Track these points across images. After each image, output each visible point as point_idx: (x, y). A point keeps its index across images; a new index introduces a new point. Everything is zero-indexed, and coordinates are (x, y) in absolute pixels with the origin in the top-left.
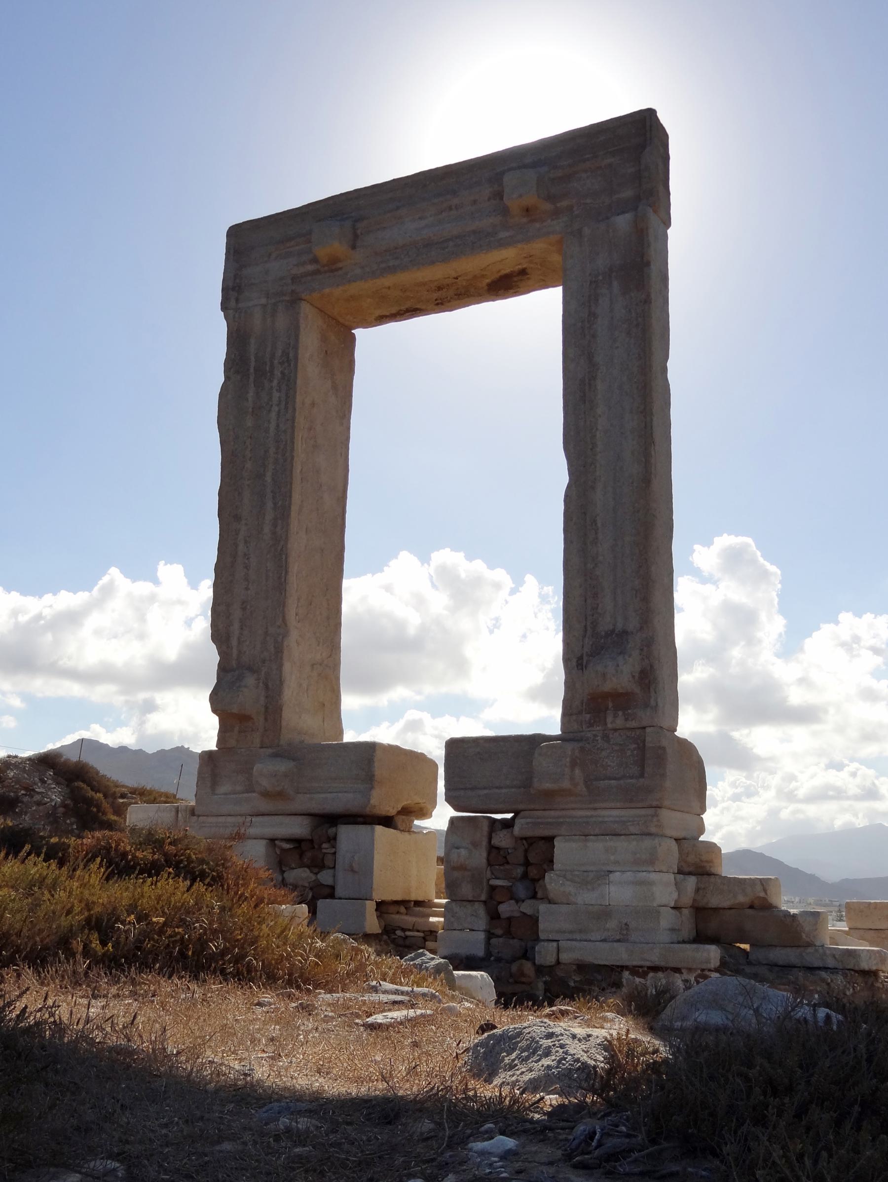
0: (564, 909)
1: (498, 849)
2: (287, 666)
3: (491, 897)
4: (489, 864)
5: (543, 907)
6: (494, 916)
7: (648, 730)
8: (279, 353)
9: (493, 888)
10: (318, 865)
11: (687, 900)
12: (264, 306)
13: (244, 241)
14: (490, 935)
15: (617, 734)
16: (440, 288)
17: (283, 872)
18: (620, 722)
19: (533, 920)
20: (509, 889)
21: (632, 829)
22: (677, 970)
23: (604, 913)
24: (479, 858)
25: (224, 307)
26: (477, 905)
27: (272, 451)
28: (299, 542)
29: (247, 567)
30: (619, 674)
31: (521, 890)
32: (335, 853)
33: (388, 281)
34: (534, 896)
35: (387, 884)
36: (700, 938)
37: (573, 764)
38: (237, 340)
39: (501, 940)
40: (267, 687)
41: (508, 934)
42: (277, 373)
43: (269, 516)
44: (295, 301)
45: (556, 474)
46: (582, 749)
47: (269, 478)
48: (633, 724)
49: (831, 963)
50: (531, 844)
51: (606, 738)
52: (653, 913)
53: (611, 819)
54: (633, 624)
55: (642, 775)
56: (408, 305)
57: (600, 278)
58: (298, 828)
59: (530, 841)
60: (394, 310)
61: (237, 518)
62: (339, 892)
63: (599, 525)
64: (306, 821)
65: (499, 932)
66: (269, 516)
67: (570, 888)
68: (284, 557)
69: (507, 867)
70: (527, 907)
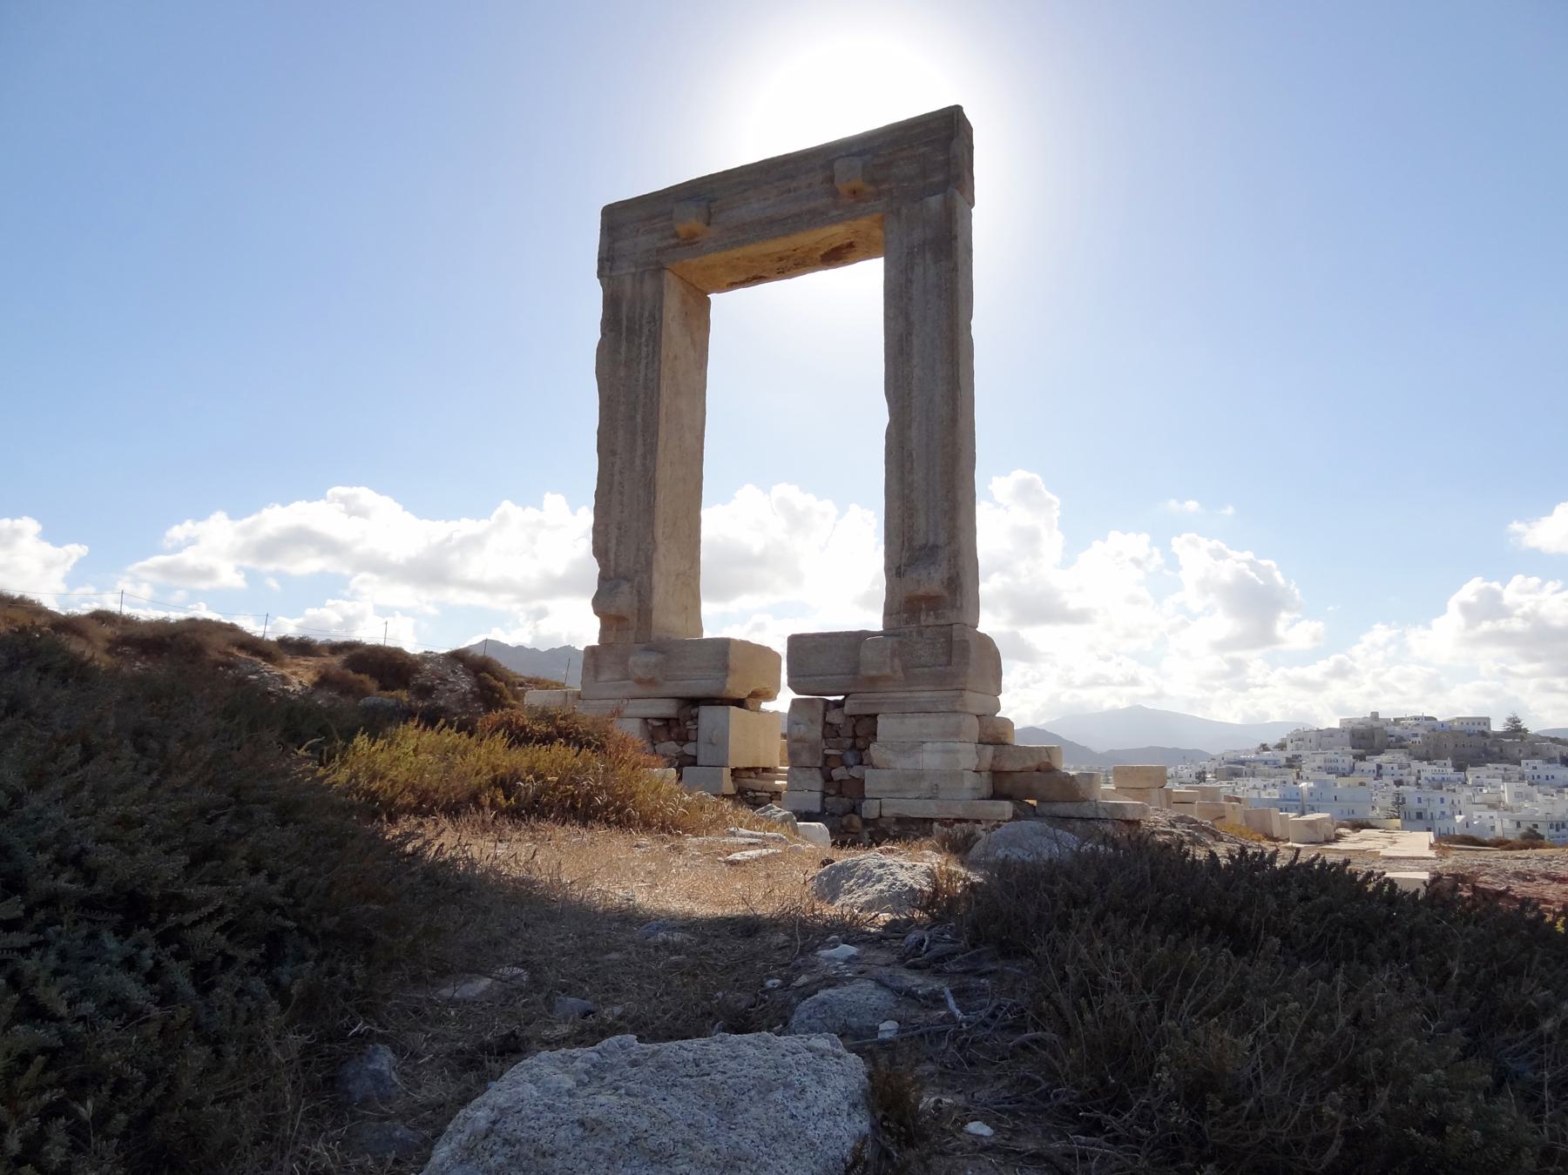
0: (886, 773)
2: (656, 577)
3: (825, 763)
4: (824, 737)
5: (868, 772)
6: (828, 779)
8: (646, 314)
9: (827, 757)
10: (683, 739)
11: (986, 764)
12: (634, 275)
13: (617, 219)
14: (825, 795)
16: (781, 259)
18: (931, 621)
19: (861, 782)
20: (840, 757)
21: (942, 708)
22: (978, 822)
23: (919, 776)
24: (816, 732)
25: (600, 275)
27: (642, 396)
28: (664, 474)
29: (621, 493)
30: (931, 581)
33: (737, 253)
34: (861, 763)
35: (740, 755)
36: (996, 795)
37: (893, 655)
38: (611, 304)
41: (840, 793)
42: (646, 330)
43: (640, 451)
44: (659, 269)
45: (878, 415)
46: (900, 643)
47: (639, 419)
48: (943, 622)
49: (1102, 815)
51: (920, 633)
52: (957, 776)
54: (942, 538)
55: (949, 663)
56: (754, 273)
58: (667, 709)
59: (858, 718)
60: (743, 278)
61: (614, 453)
64: (673, 703)
65: (832, 792)
66: (640, 451)
70: (855, 772)
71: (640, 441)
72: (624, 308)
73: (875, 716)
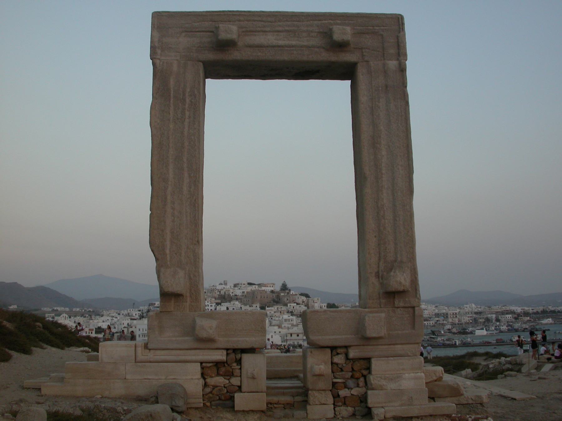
1: (337, 364)
4: (333, 372)
5: (369, 392)
6: (336, 396)
7: (416, 308)
8: (188, 90)
9: (334, 384)
13: (163, 22)
15: (399, 310)
17: (204, 379)
18: (401, 304)
20: (344, 382)
26: (327, 392)
29: (173, 209)
31: (351, 383)
32: (240, 369)
34: (358, 386)
39: (342, 408)
40: (190, 279)
41: (345, 404)
42: (188, 100)
47: (185, 160)
50: (354, 362)
53: (399, 348)
57: (380, 89)
62: (244, 388)
63: (385, 209)
65: (340, 404)
67: (383, 382)
68: (197, 205)
69: (343, 373)
70: (355, 391)
71: (186, 175)
72: (172, 82)
73: (368, 360)
